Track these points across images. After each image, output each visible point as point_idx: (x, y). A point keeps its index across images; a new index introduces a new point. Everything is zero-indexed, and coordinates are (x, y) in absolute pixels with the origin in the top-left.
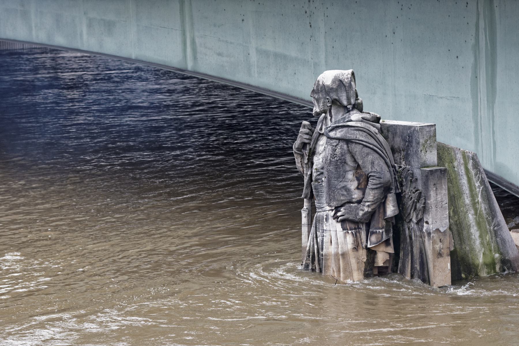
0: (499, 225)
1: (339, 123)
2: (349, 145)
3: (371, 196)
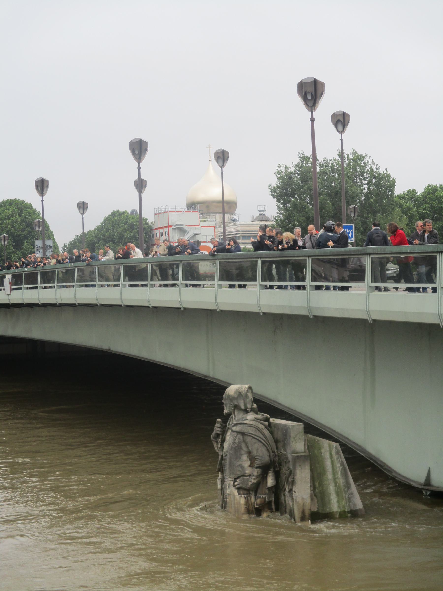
0: (352, 494)
1: (239, 421)
2: (244, 437)
3: (256, 472)
